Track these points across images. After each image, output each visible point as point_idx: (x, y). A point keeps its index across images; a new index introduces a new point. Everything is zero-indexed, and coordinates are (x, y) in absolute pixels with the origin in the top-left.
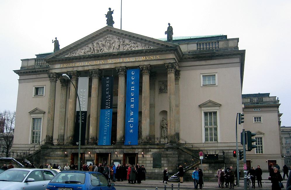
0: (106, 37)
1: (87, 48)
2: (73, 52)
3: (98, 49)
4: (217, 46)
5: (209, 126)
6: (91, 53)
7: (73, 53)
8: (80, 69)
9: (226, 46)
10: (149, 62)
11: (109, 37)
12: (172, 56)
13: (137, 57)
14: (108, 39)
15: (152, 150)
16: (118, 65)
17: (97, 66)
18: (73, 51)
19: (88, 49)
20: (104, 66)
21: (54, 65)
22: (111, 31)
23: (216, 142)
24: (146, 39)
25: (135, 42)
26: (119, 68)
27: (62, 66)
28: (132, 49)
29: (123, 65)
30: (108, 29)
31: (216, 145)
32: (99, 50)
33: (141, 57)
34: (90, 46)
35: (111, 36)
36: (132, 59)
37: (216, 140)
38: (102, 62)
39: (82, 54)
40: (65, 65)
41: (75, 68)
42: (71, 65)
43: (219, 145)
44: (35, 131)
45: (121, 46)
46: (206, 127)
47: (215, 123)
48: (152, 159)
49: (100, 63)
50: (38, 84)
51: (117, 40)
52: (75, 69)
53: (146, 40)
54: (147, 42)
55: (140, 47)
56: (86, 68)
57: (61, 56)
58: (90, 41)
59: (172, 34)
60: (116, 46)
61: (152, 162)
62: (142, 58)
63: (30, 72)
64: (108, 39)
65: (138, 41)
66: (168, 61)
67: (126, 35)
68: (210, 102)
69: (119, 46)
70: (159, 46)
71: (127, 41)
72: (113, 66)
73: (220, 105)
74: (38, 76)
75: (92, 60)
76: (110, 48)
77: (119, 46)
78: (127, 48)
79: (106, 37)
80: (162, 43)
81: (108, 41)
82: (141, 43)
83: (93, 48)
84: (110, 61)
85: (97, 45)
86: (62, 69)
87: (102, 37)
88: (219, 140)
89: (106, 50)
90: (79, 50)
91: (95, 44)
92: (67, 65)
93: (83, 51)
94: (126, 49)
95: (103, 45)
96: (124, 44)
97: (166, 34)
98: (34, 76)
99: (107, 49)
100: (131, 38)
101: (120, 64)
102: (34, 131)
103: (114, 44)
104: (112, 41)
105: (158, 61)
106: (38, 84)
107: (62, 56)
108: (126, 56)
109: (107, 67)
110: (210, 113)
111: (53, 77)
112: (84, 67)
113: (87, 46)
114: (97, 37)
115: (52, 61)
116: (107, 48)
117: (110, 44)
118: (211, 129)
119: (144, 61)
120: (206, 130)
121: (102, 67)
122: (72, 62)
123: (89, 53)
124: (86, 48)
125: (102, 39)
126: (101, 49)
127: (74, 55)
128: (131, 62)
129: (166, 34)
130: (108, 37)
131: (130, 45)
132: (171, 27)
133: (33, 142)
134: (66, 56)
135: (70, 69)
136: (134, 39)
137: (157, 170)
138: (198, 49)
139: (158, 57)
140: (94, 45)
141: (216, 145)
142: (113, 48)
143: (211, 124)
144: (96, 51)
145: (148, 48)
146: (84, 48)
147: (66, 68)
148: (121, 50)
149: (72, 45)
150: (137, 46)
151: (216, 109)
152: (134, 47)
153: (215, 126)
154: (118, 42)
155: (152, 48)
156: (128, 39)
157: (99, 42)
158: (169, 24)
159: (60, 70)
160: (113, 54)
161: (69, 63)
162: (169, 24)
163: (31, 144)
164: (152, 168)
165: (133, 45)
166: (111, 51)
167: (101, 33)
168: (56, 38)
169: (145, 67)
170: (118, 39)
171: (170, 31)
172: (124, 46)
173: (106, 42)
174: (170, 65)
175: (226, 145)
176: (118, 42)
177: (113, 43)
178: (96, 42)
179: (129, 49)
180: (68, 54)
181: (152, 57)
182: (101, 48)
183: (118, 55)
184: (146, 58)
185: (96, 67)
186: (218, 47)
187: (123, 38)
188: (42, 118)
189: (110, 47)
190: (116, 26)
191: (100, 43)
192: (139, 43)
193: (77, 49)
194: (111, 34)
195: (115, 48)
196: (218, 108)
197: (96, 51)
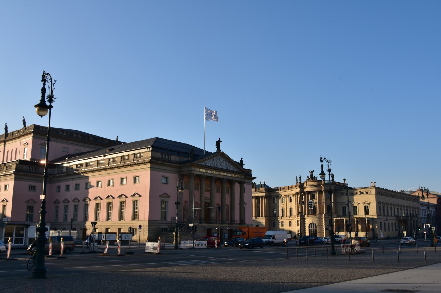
12: (243, 177)
29: (226, 177)
39: (209, 165)
45: (226, 165)
51: (224, 161)
55: (232, 168)
65: (232, 165)
72: (222, 177)
82: (233, 166)
89: (219, 166)
91: (215, 160)
140: (214, 161)
146: (209, 161)
147: (201, 172)
155: (238, 171)
157: (217, 160)
158: (242, 158)
162: (242, 158)
180: (202, 163)
194: (222, 156)
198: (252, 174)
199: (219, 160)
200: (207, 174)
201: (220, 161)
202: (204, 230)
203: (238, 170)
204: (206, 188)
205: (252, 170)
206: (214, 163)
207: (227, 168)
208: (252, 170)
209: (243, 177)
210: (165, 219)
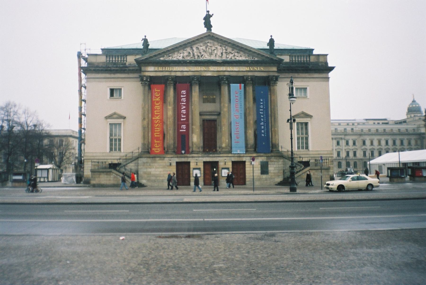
0: (207, 42)
1: (186, 51)
2: (170, 55)
3: (199, 54)
4: (308, 60)
5: (301, 136)
6: (190, 58)
7: (170, 56)
8: (179, 74)
9: (316, 61)
10: (253, 73)
11: (210, 43)
12: (275, 69)
13: (240, 67)
14: (209, 44)
15: (260, 158)
16: (222, 74)
17: (199, 73)
18: (169, 54)
19: (186, 54)
20: (206, 73)
21: (147, 67)
22: (213, 36)
23: (307, 150)
24: (251, 50)
25: (239, 51)
26: (223, 77)
27: (156, 69)
28: (236, 58)
29: (227, 74)
30: (210, 34)
31: (308, 152)
32: (200, 56)
33: (244, 67)
34: (189, 50)
35: (211, 41)
36: (236, 69)
37: (307, 148)
38: (203, 68)
39: (181, 58)
40: (160, 69)
41: (172, 73)
42: (167, 69)
43: (311, 153)
44: (114, 137)
45: (224, 54)
46: (298, 136)
47: (307, 133)
48: (260, 166)
49: (201, 70)
50: (115, 85)
52: (173, 74)
53: (250, 51)
54: (251, 53)
56: (186, 74)
57: (154, 58)
58: (189, 45)
59: (274, 46)
60: (219, 54)
61: (260, 169)
62: (247, 69)
63: (102, 70)
64: (209, 44)
65: (242, 51)
66: (271, 74)
67: (230, 43)
68: (303, 113)
69: (222, 53)
70: (264, 58)
71: (229, 50)
72: (215, 74)
73: (310, 116)
74: (113, 76)
75: (193, 66)
76: (211, 54)
77: (222, 53)
78: (230, 57)
79: (207, 42)
80: (267, 56)
81: (209, 47)
82: (245, 53)
83: (193, 53)
84: (212, 68)
85: (196, 50)
86: (157, 73)
87: (202, 42)
88: (310, 148)
89: (206, 57)
90: (176, 53)
91: (194, 49)
92: (163, 68)
93: (182, 55)
94: (230, 57)
95: (204, 51)
96: (227, 51)
97: (268, 46)
98: (108, 75)
99: (208, 55)
100: (234, 47)
101: (223, 73)
102: (111, 138)
103: (216, 51)
104: (213, 48)
105: (262, 73)
106: (115, 85)
107: (156, 57)
108: (230, 64)
109: (209, 74)
110: (302, 123)
111: (146, 80)
112: (183, 73)
113: (185, 49)
114: (197, 42)
115: (145, 63)
116: (208, 54)
117: (211, 50)
118: (302, 138)
119: (249, 71)
120: (298, 139)
121: (203, 74)
122: (169, 66)
123: (189, 58)
124: (185, 52)
125: (201, 44)
126: (202, 55)
127: (170, 58)
128: (235, 71)
129: (268, 46)
130: (208, 43)
131: (233, 54)
132: (273, 39)
133: (111, 149)
134: (162, 59)
135: (167, 73)
136: (238, 48)
137: (264, 176)
138: (290, 61)
139: (262, 69)
140: (193, 50)
141: (308, 152)
142: (215, 55)
143: (302, 134)
144: (196, 57)
145: (252, 58)
146: (181, 51)
147: (162, 71)
148: (224, 58)
149: (169, 48)
150: (241, 56)
151: (307, 120)
152: (237, 56)
153: (306, 136)
154: (220, 49)
155: (256, 59)
156: (230, 47)
157: (199, 47)
158: (271, 36)
159: (154, 73)
160: (218, 61)
161: (165, 66)
162: (271, 36)
163: (110, 152)
164: (260, 174)
165: (236, 54)
166: (213, 58)
167: (202, 38)
168: (145, 36)
169: (249, 77)
170: (221, 46)
171: (271, 42)
172: (227, 54)
173: (206, 48)
174: (274, 78)
175: (317, 153)
176: (220, 49)
177: (214, 50)
178: (196, 46)
179: (233, 58)
180: (163, 56)
181: (256, 69)
182: (202, 54)
183: (222, 63)
184: (250, 68)
185: (197, 74)
186: (309, 61)
187: (226, 45)
188: (122, 124)
189: (211, 54)
190: (214, 30)
191: (201, 48)
192: (242, 53)
193: (174, 52)
195: (217, 56)
196: (309, 119)
197: (196, 57)
198: (329, 61)
199: (206, 48)
200: (177, 73)
201: (209, 49)
202: (169, 164)
203: (256, 57)
204: (205, 97)
205: (327, 55)
206: (193, 55)
207: (228, 58)
208: (327, 55)
209: (275, 69)
210: (120, 149)
